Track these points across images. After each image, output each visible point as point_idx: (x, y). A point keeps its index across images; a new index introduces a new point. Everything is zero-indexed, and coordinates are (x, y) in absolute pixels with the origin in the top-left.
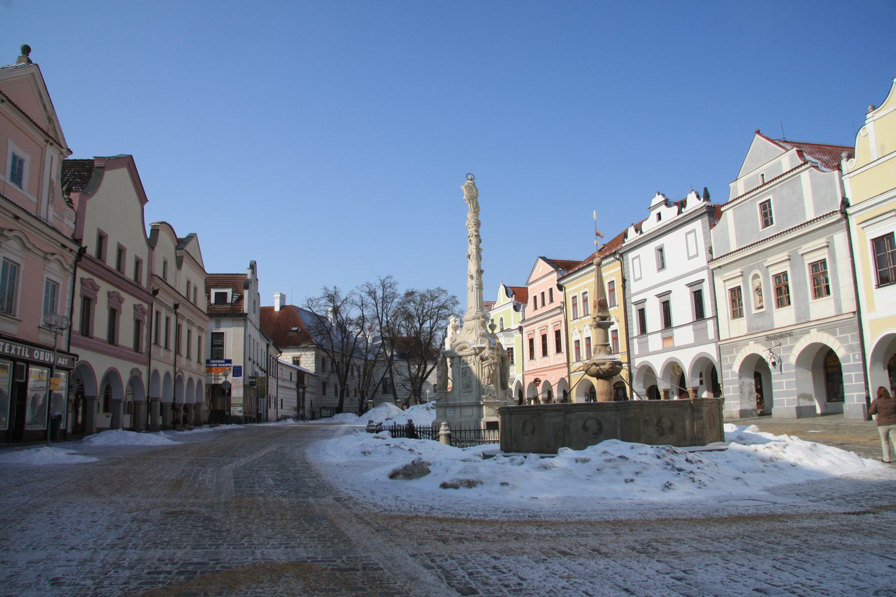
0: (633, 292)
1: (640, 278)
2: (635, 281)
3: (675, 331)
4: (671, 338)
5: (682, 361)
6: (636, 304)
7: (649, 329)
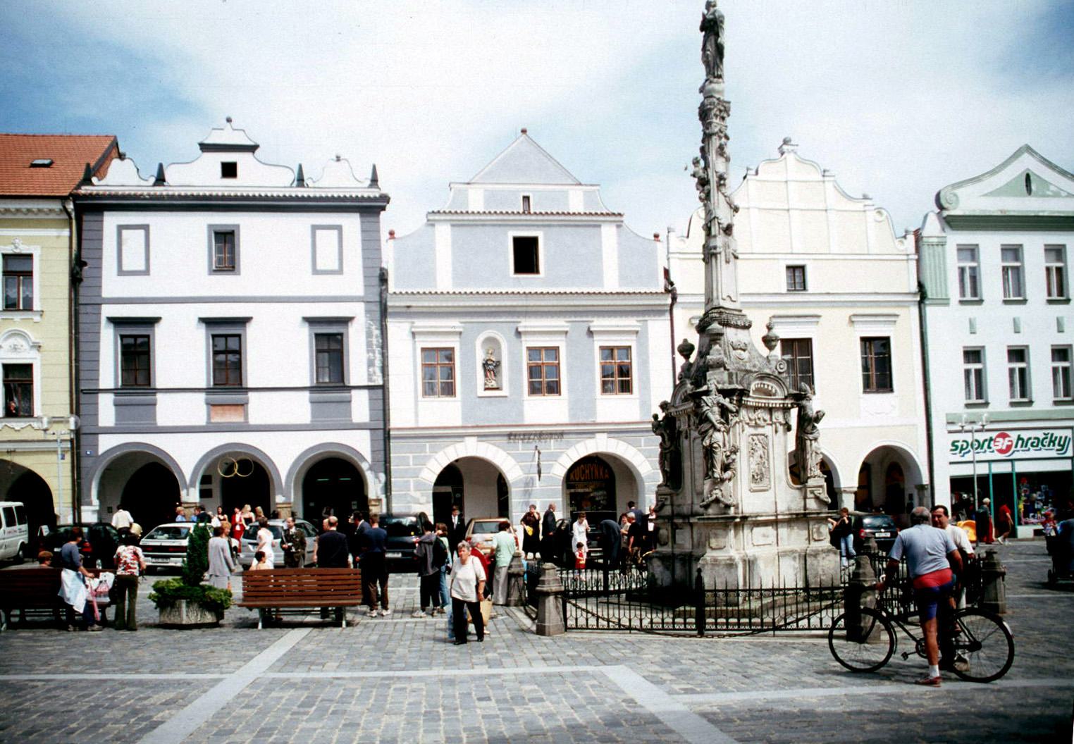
0: (106, 292)
1: (146, 272)
2: (121, 272)
3: (251, 394)
4: (243, 405)
5: (298, 453)
6: (117, 322)
7: (161, 377)
